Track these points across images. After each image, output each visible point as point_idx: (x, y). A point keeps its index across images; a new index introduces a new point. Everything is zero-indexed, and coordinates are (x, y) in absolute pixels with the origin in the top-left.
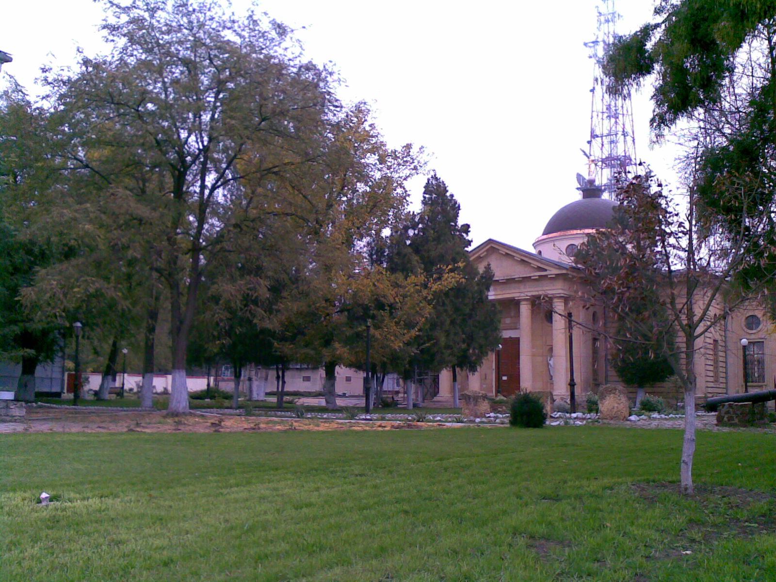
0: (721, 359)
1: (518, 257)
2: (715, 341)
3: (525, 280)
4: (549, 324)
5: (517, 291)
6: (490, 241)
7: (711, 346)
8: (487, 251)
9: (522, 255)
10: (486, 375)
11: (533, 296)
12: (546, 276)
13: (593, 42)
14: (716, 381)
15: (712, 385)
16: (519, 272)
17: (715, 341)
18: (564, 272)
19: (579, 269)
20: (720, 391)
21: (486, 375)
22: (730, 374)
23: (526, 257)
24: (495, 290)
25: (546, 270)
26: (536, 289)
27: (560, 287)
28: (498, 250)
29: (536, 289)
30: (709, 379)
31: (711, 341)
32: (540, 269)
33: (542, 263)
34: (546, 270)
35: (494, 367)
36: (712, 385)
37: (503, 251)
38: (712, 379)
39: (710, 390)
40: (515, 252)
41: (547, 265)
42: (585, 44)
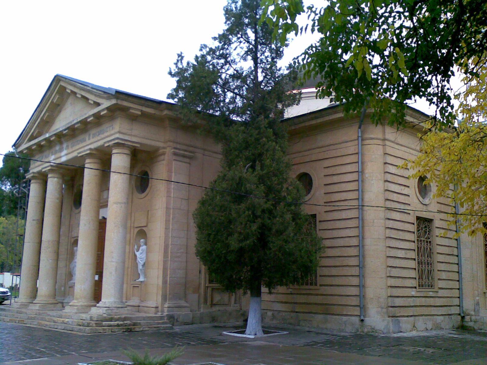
11: (96, 149)
15: (413, 293)
22: (466, 274)
31: (414, 220)
36: (413, 293)
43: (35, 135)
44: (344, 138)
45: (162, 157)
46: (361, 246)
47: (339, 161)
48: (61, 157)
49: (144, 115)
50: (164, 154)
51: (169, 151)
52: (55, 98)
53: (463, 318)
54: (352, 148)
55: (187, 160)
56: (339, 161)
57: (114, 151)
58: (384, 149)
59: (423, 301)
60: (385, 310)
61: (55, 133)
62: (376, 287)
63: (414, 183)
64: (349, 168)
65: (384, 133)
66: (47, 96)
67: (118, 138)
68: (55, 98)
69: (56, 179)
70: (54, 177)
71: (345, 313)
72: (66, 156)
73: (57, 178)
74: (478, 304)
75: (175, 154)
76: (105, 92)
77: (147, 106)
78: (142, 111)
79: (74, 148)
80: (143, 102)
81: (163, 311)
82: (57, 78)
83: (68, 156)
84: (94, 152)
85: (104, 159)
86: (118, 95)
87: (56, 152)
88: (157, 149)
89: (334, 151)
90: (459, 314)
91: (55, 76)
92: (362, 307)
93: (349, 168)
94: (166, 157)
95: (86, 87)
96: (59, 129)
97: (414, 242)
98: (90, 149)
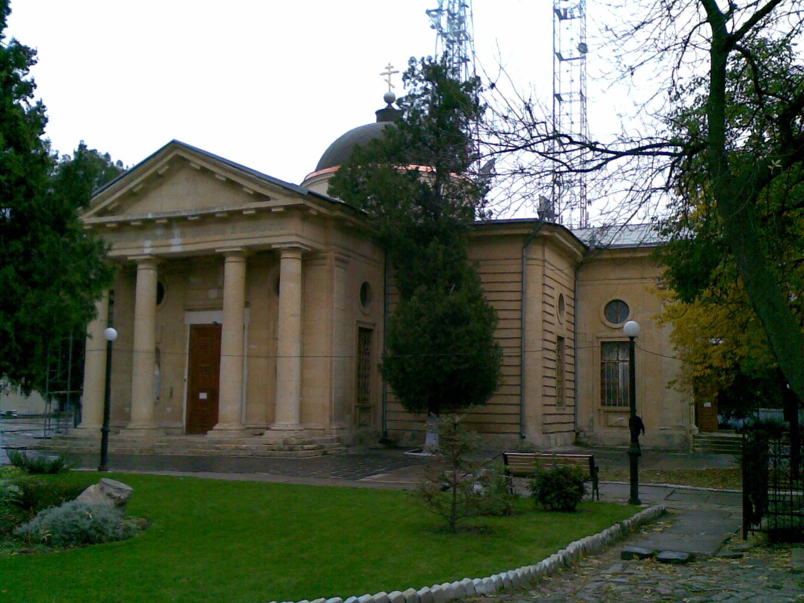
0: (568, 368)
1: (221, 175)
2: (560, 339)
3: (233, 216)
5: (220, 237)
6: (174, 145)
7: (553, 347)
8: (170, 163)
9: (226, 170)
10: (172, 389)
11: (248, 248)
12: (268, 210)
13: (436, 11)
14: (560, 404)
15: (553, 410)
16: (223, 201)
17: (560, 339)
18: (300, 201)
19: (335, 203)
20: (565, 419)
21: (172, 389)
22: (580, 392)
23: (235, 174)
24: (183, 235)
25: (267, 198)
26: (251, 235)
27: (293, 231)
28: (188, 161)
29: (251, 235)
30: (549, 401)
31: (554, 339)
33: (261, 186)
34: (267, 198)
35: (186, 377)
36: (553, 410)
37: (197, 163)
38: (553, 401)
39: (549, 419)
40: (215, 165)
41: (272, 190)
42: (428, 12)
43: (110, 208)
46: (521, 366)
47: (499, 278)
48: (170, 246)
49: (320, 216)
50: (324, 258)
51: (331, 255)
53: (577, 434)
54: (515, 267)
56: (499, 278)
57: (283, 256)
58: (544, 270)
59: (558, 418)
60: (540, 427)
61: (169, 215)
62: (536, 405)
63: (555, 302)
65: (543, 254)
67: (297, 243)
69: (152, 272)
70: (150, 269)
71: (503, 430)
74: (592, 420)
75: (337, 259)
76: (286, 188)
77: (323, 206)
78: (318, 211)
80: (321, 201)
81: (330, 434)
84: (244, 250)
85: (262, 263)
86: (310, 196)
90: (574, 431)
92: (521, 425)
95: (244, 173)
96: (179, 212)
97: (555, 361)
98: (241, 247)
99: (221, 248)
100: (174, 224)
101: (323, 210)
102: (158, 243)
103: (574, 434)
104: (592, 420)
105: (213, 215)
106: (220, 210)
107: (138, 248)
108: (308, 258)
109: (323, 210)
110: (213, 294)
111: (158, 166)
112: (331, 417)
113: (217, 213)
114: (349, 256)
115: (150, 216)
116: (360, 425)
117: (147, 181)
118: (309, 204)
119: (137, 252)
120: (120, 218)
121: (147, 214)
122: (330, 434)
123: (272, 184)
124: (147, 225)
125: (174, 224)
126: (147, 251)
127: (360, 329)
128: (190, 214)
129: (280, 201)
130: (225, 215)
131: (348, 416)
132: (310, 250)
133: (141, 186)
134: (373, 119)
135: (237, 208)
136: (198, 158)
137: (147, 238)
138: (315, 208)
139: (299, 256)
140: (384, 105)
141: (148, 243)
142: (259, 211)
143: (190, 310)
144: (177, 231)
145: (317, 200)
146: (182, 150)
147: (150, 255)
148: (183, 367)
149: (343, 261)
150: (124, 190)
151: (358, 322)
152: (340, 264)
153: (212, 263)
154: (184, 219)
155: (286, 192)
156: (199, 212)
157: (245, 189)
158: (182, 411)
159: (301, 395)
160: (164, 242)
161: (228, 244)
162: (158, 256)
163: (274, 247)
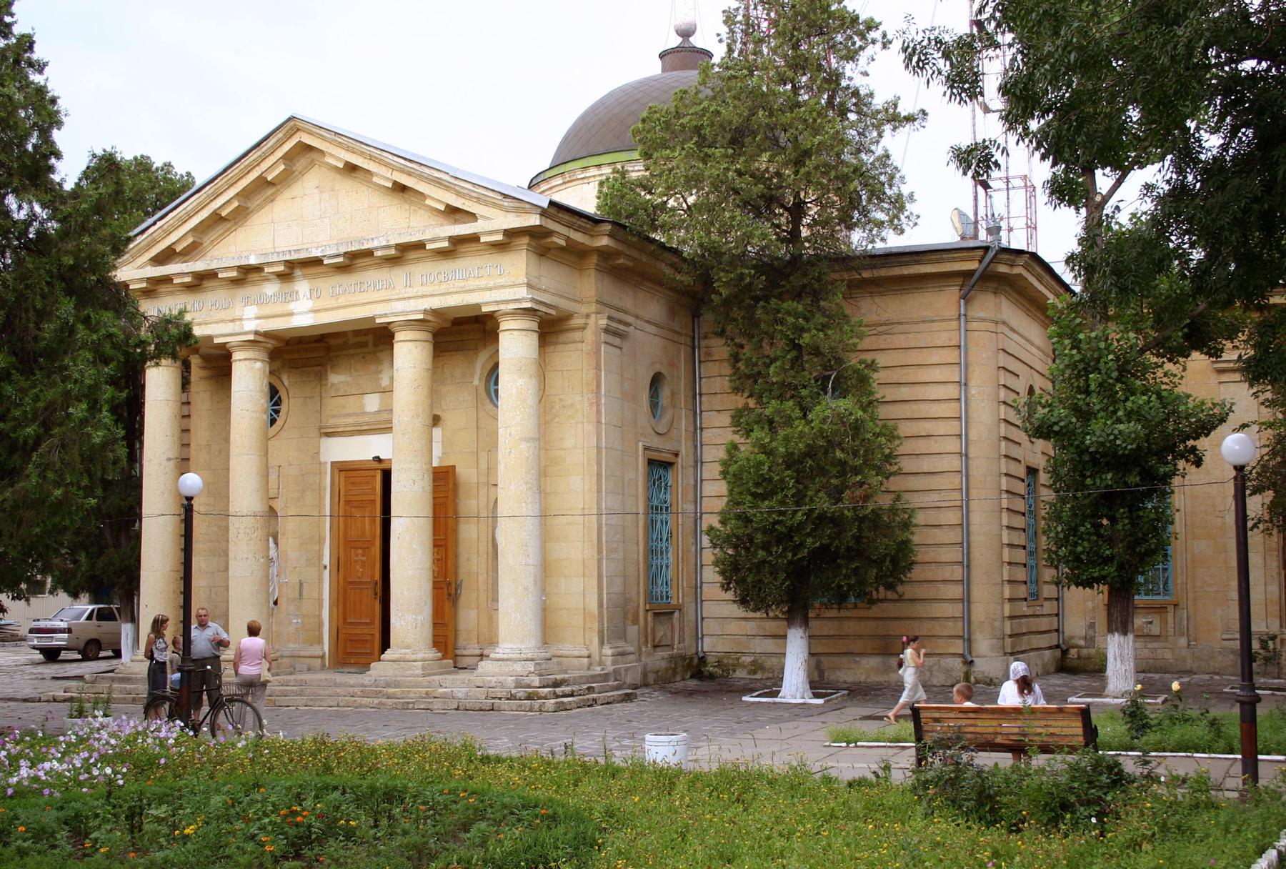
2: (1032, 471)
3: (405, 253)
4: (489, 406)
11: (435, 312)
12: (474, 239)
15: (1024, 608)
16: (390, 224)
18: (534, 220)
20: (1043, 624)
25: (472, 217)
31: (1020, 471)
32: (453, 212)
33: (458, 194)
34: (472, 217)
35: (326, 561)
40: (371, 158)
41: (479, 200)
44: (926, 313)
45: (577, 335)
47: (914, 357)
48: (291, 314)
52: (271, 166)
53: (1065, 652)
54: (946, 334)
55: (617, 341)
61: (288, 258)
64: (937, 374)
66: (246, 162)
68: (271, 166)
69: (259, 364)
72: (311, 315)
73: (263, 361)
75: (607, 331)
76: (506, 196)
78: (568, 239)
79: (342, 301)
82: (292, 123)
83: (318, 315)
84: (429, 318)
86: (553, 211)
87: (262, 301)
88: (569, 316)
89: (902, 336)
90: (1058, 646)
91: (292, 118)
93: (937, 374)
94: (589, 335)
95: (426, 170)
97: (1024, 514)
98: (425, 312)
99: (386, 315)
100: (298, 272)
101: (577, 237)
102: (268, 310)
103: (1058, 653)
104: (1092, 626)
105: (369, 253)
106: (384, 243)
107: (233, 321)
108: (550, 328)
109: (577, 237)
110: (372, 403)
111: (264, 166)
112: (601, 632)
113: (376, 249)
114: (628, 324)
115: (253, 261)
116: (655, 647)
117: (246, 194)
118: (551, 225)
119: (229, 328)
120: (200, 266)
121: (247, 257)
122: (601, 663)
123: (481, 191)
124: (247, 274)
125: (298, 272)
126: (251, 326)
127: (651, 462)
128: (328, 253)
129: (494, 222)
130: (393, 252)
131: (633, 631)
132: (553, 312)
133: (236, 204)
134: (654, 68)
135: (414, 239)
136: (340, 145)
137: (248, 302)
138: (562, 233)
139: (535, 326)
140: (676, 41)
141: (251, 311)
142: (458, 245)
143: (328, 435)
144: (302, 286)
145: (566, 217)
146: (311, 133)
147: (256, 333)
148: (321, 541)
149: (616, 333)
150: (205, 214)
151: (646, 449)
152: (610, 339)
153: (372, 341)
154: (317, 262)
155: (506, 203)
156: (343, 250)
157: (428, 202)
158: (321, 625)
159: (543, 590)
160: (279, 309)
161: (399, 306)
162: (268, 335)
163: (485, 309)
